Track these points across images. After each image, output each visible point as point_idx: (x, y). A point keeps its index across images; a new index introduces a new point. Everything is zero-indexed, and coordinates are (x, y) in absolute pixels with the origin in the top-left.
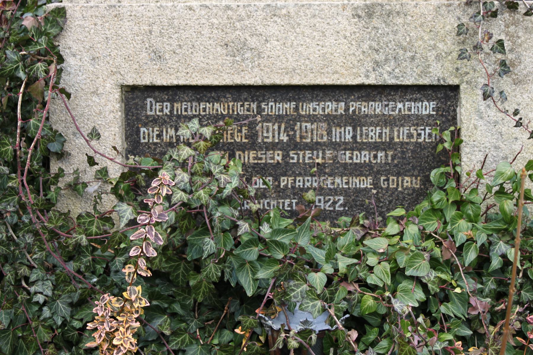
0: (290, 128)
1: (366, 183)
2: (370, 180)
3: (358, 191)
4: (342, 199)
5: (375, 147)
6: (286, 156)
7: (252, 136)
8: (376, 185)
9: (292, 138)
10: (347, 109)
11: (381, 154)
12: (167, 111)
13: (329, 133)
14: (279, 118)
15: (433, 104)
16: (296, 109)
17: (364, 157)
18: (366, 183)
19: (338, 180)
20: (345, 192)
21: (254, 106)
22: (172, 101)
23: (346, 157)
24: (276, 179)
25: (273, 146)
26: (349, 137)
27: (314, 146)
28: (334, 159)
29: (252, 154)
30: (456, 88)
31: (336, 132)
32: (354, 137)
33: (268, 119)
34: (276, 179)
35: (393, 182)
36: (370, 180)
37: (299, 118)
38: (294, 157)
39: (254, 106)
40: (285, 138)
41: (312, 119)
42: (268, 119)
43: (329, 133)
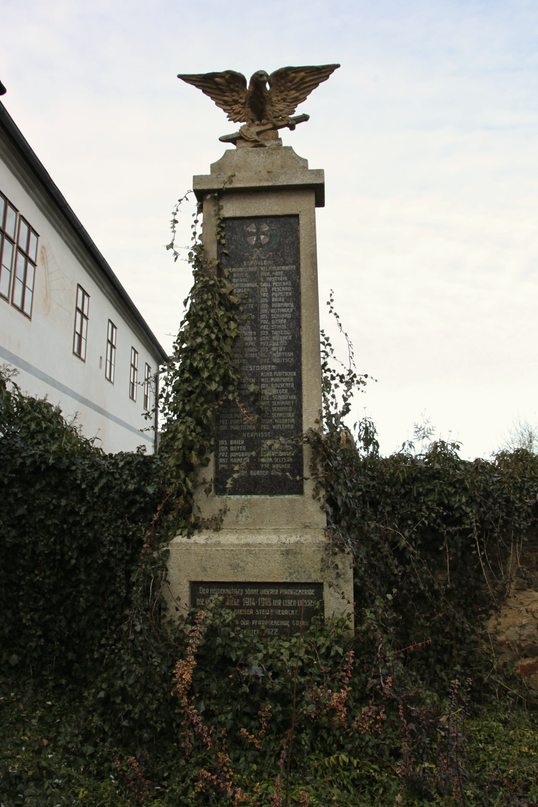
0: (256, 600)
1: (286, 623)
2: (288, 622)
4: (277, 630)
5: (290, 608)
6: (254, 612)
7: (241, 603)
8: (291, 624)
9: (257, 604)
10: (279, 592)
11: (292, 611)
12: (207, 592)
13: (272, 602)
14: (252, 596)
15: (313, 591)
16: (259, 592)
17: (286, 612)
18: (286, 623)
19: (275, 622)
21: (242, 590)
22: (210, 588)
23: (279, 612)
24: (251, 621)
25: (249, 607)
26: (280, 604)
27: (266, 608)
28: (274, 613)
29: (241, 611)
31: (275, 602)
32: (282, 604)
33: (247, 596)
34: (251, 621)
36: (288, 622)
37: (260, 596)
38: (258, 612)
39: (242, 590)
40: (254, 604)
41: (265, 596)
42: (247, 596)
43: (272, 602)
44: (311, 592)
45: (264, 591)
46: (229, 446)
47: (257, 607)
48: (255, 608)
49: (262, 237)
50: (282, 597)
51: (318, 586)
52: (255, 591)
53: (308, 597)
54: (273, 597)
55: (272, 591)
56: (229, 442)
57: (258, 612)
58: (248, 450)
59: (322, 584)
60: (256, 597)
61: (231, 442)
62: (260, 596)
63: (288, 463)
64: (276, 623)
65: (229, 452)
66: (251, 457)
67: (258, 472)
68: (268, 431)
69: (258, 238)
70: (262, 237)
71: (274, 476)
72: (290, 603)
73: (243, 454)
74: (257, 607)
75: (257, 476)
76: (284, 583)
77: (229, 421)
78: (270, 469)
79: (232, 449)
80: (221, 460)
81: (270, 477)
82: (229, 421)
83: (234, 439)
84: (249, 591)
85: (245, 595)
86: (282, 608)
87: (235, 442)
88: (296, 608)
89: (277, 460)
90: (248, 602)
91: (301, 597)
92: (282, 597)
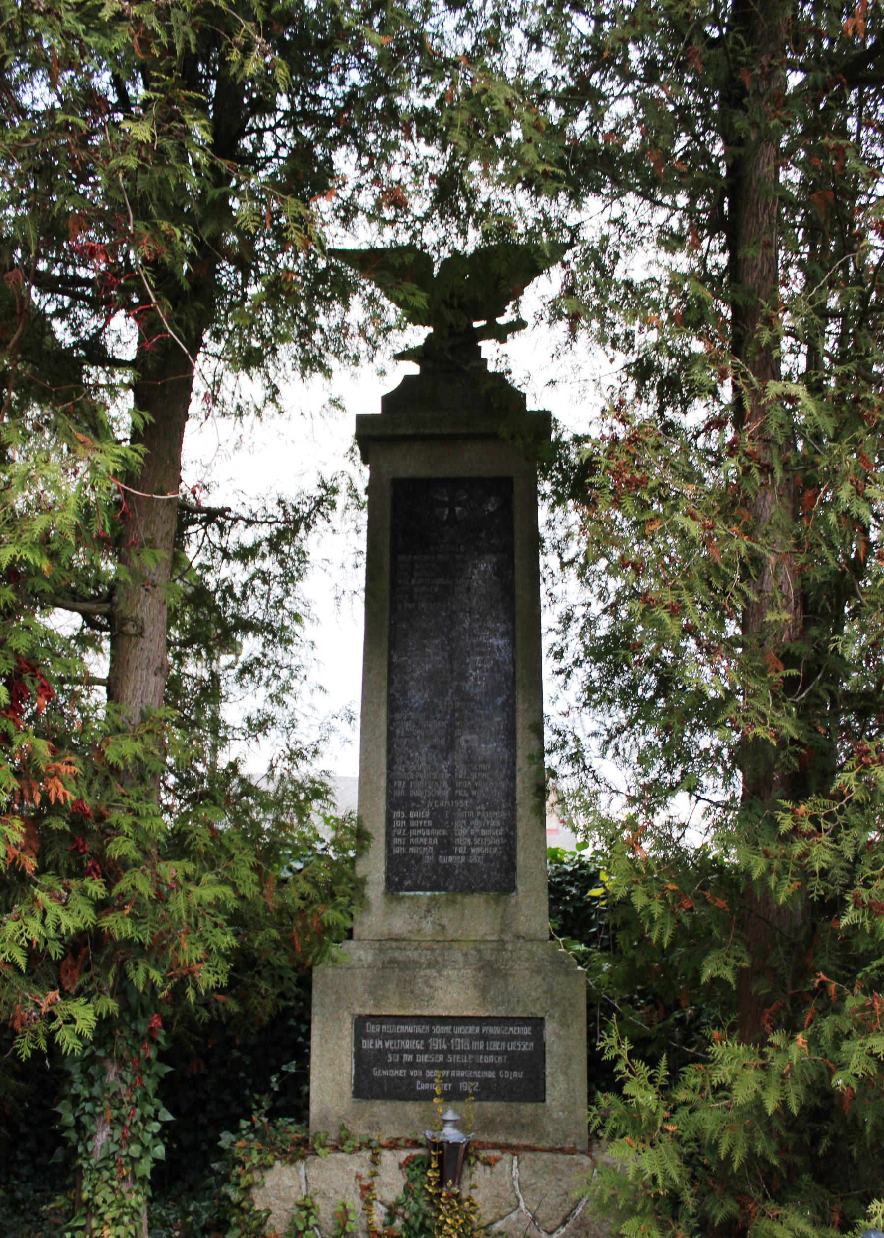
0: (448, 1041)
1: (491, 1074)
3: (487, 1080)
5: (496, 1053)
6: (446, 1058)
7: (426, 1046)
8: (497, 1075)
14: (442, 1036)
17: (490, 1059)
18: (491, 1074)
20: (479, 1080)
22: (381, 1024)
23: (481, 1059)
25: (439, 1052)
27: (462, 1052)
30: (542, 1019)
31: (475, 1043)
33: (436, 1036)
35: (506, 1074)
37: (453, 1036)
38: (450, 1059)
41: (461, 1036)
42: (436, 1036)
44: (527, 1031)
45: (459, 1030)
46: (407, 820)
47: (449, 1051)
48: (445, 1053)
49: (458, 509)
50: (485, 1038)
51: (537, 1023)
52: (447, 1029)
53: (523, 1038)
54: (471, 1037)
55: (472, 1029)
56: (407, 814)
57: (450, 1059)
58: (436, 826)
59: (542, 1019)
60: (448, 1038)
61: (411, 814)
62: (453, 1036)
63: (493, 845)
64: (477, 1074)
65: (408, 828)
66: (441, 838)
67: (451, 859)
68: (464, 798)
69: (452, 511)
70: (458, 509)
71: (475, 864)
72: (496, 1046)
73: (428, 832)
74: (449, 1051)
75: (450, 864)
76: (489, 1017)
77: (408, 784)
78: (468, 854)
79: (412, 824)
80: (396, 841)
81: (468, 866)
82: (408, 784)
83: (416, 809)
84: (438, 1029)
85: (431, 1034)
86: (486, 1053)
87: (417, 814)
88: (505, 1052)
89: (477, 841)
90: (437, 1044)
91: (512, 1038)
92: (485, 1038)
